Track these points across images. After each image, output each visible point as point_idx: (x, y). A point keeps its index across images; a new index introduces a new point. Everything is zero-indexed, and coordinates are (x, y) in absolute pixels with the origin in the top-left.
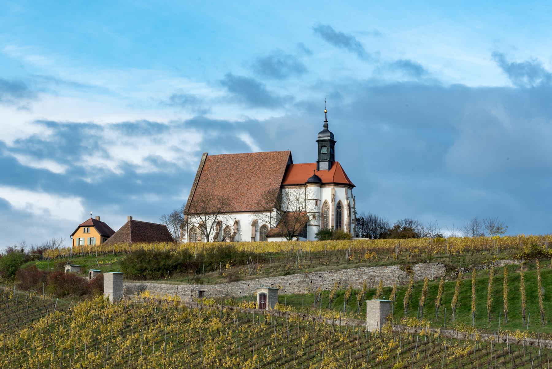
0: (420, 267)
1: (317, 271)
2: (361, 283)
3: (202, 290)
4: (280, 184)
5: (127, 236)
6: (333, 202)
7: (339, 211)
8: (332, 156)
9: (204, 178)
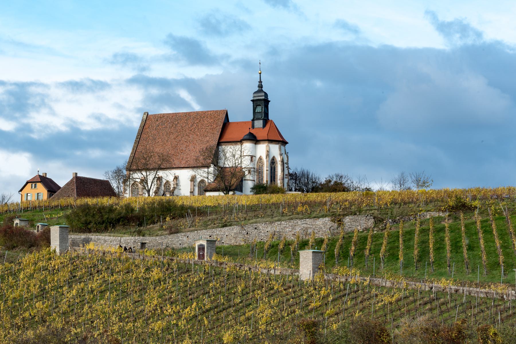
0: (350, 219)
1: (253, 223)
2: (294, 234)
3: (144, 241)
4: (217, 142)
5: (73, 191)
6: (268, 158)
7: (273, 167)
8: (267, 114)
9: (145, 136)
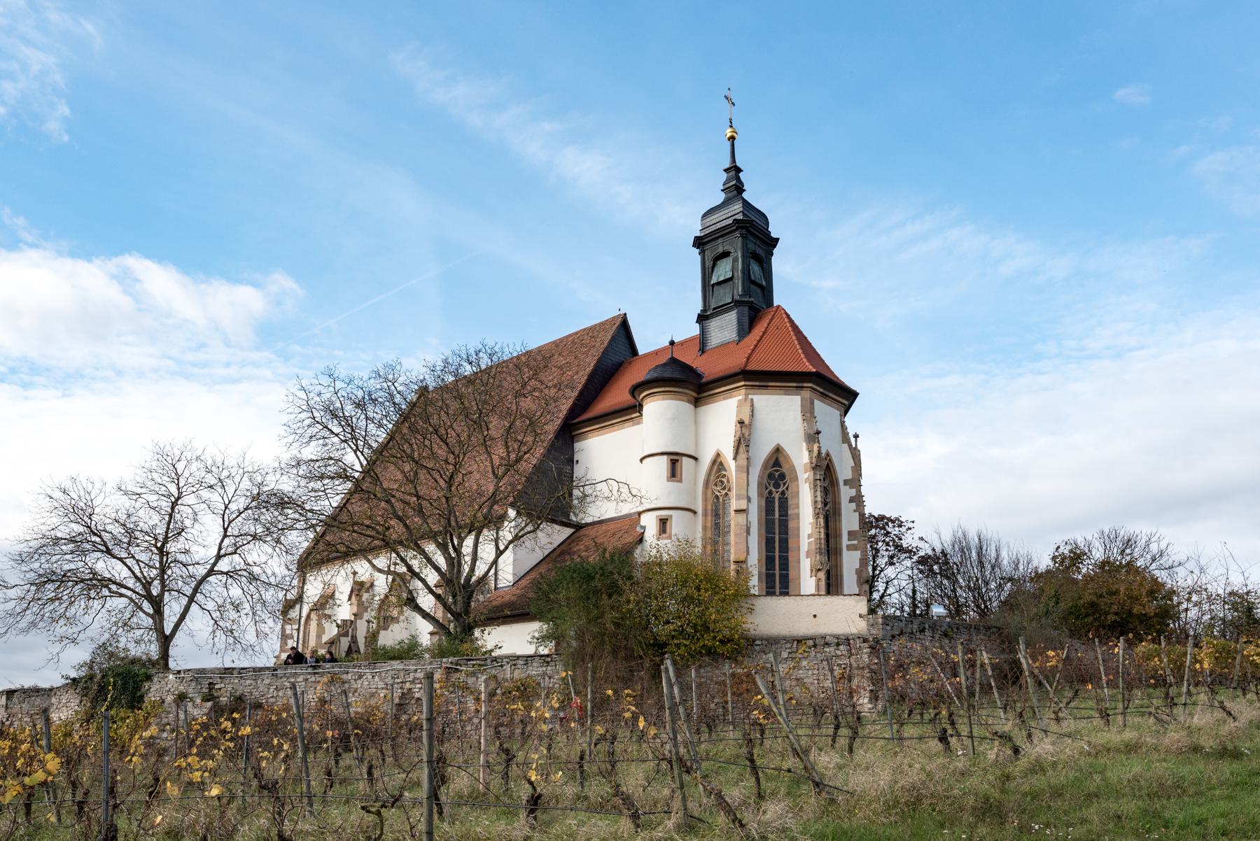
7: (777, 496)
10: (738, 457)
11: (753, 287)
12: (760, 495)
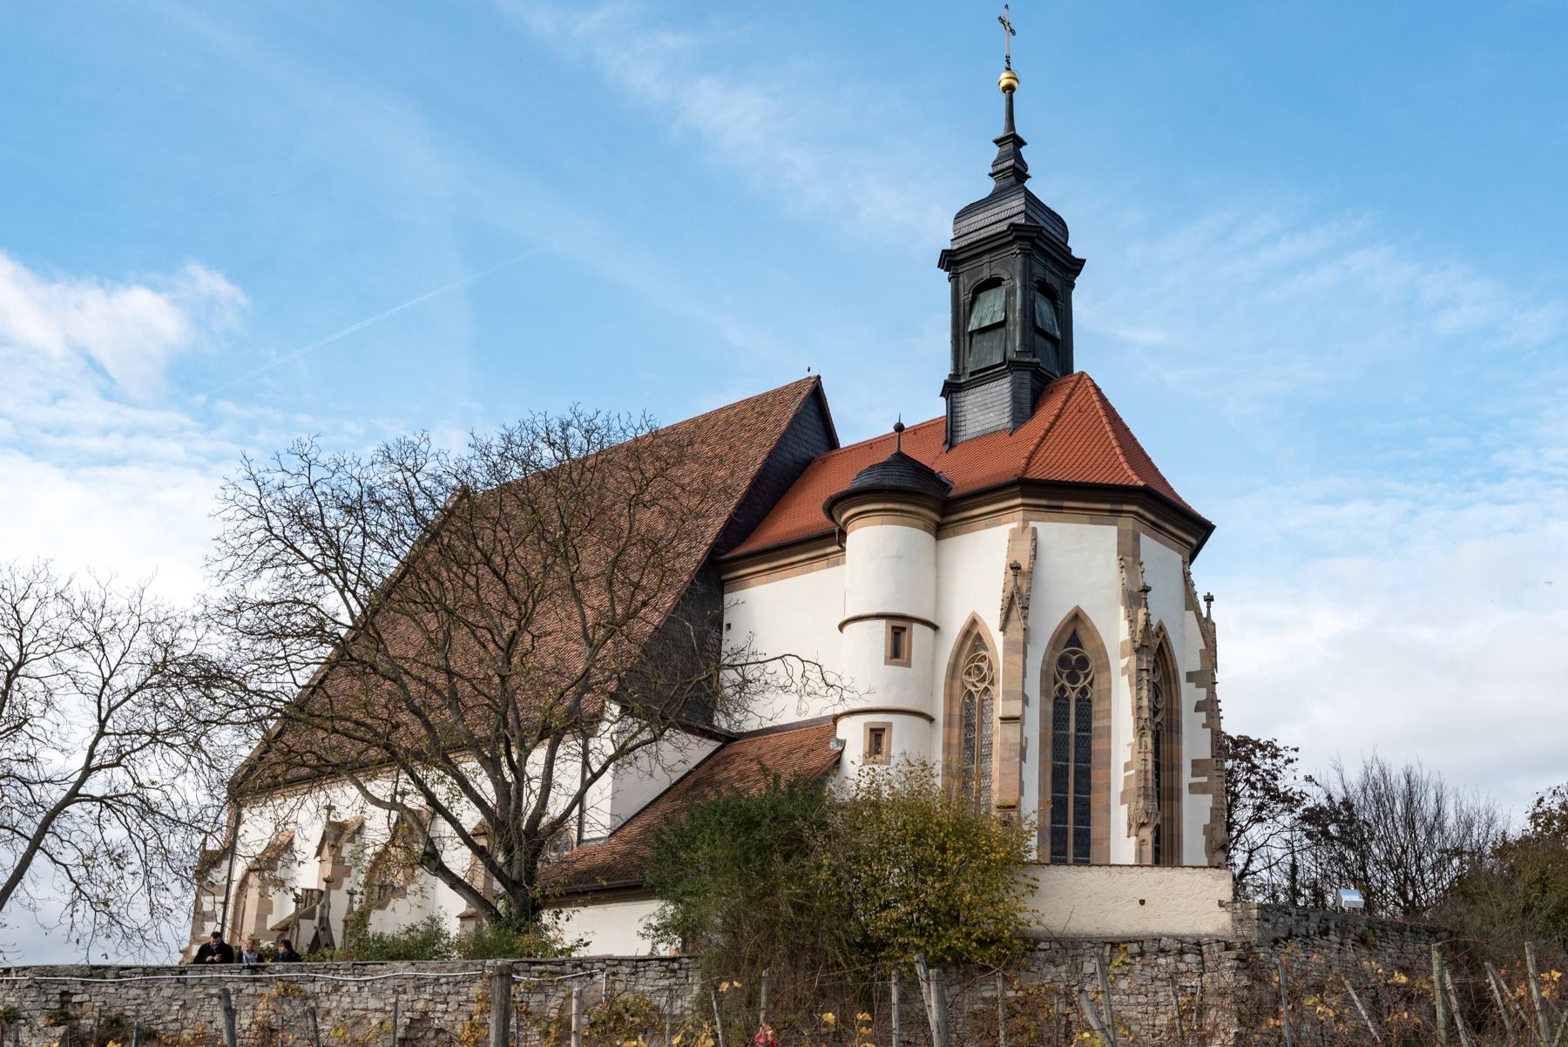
6: (1016, 625)
7: (1073, 696)
10: (1010, 627)
11: (1039, 340)
12: (1044, 692)
